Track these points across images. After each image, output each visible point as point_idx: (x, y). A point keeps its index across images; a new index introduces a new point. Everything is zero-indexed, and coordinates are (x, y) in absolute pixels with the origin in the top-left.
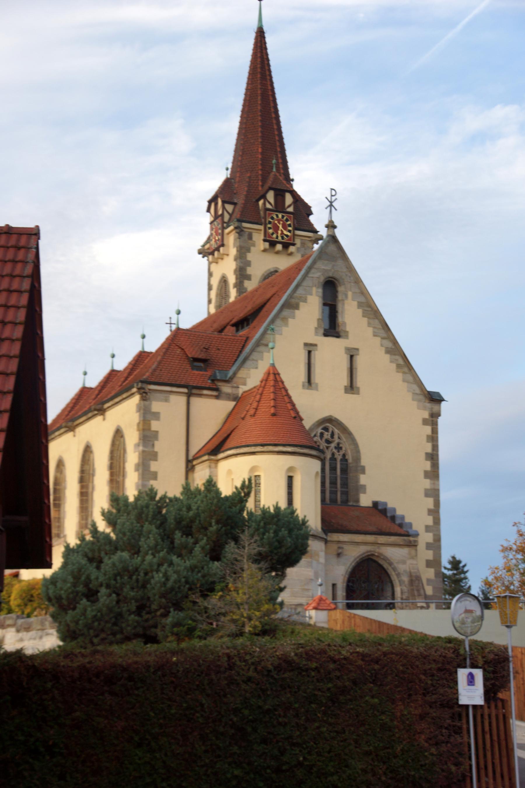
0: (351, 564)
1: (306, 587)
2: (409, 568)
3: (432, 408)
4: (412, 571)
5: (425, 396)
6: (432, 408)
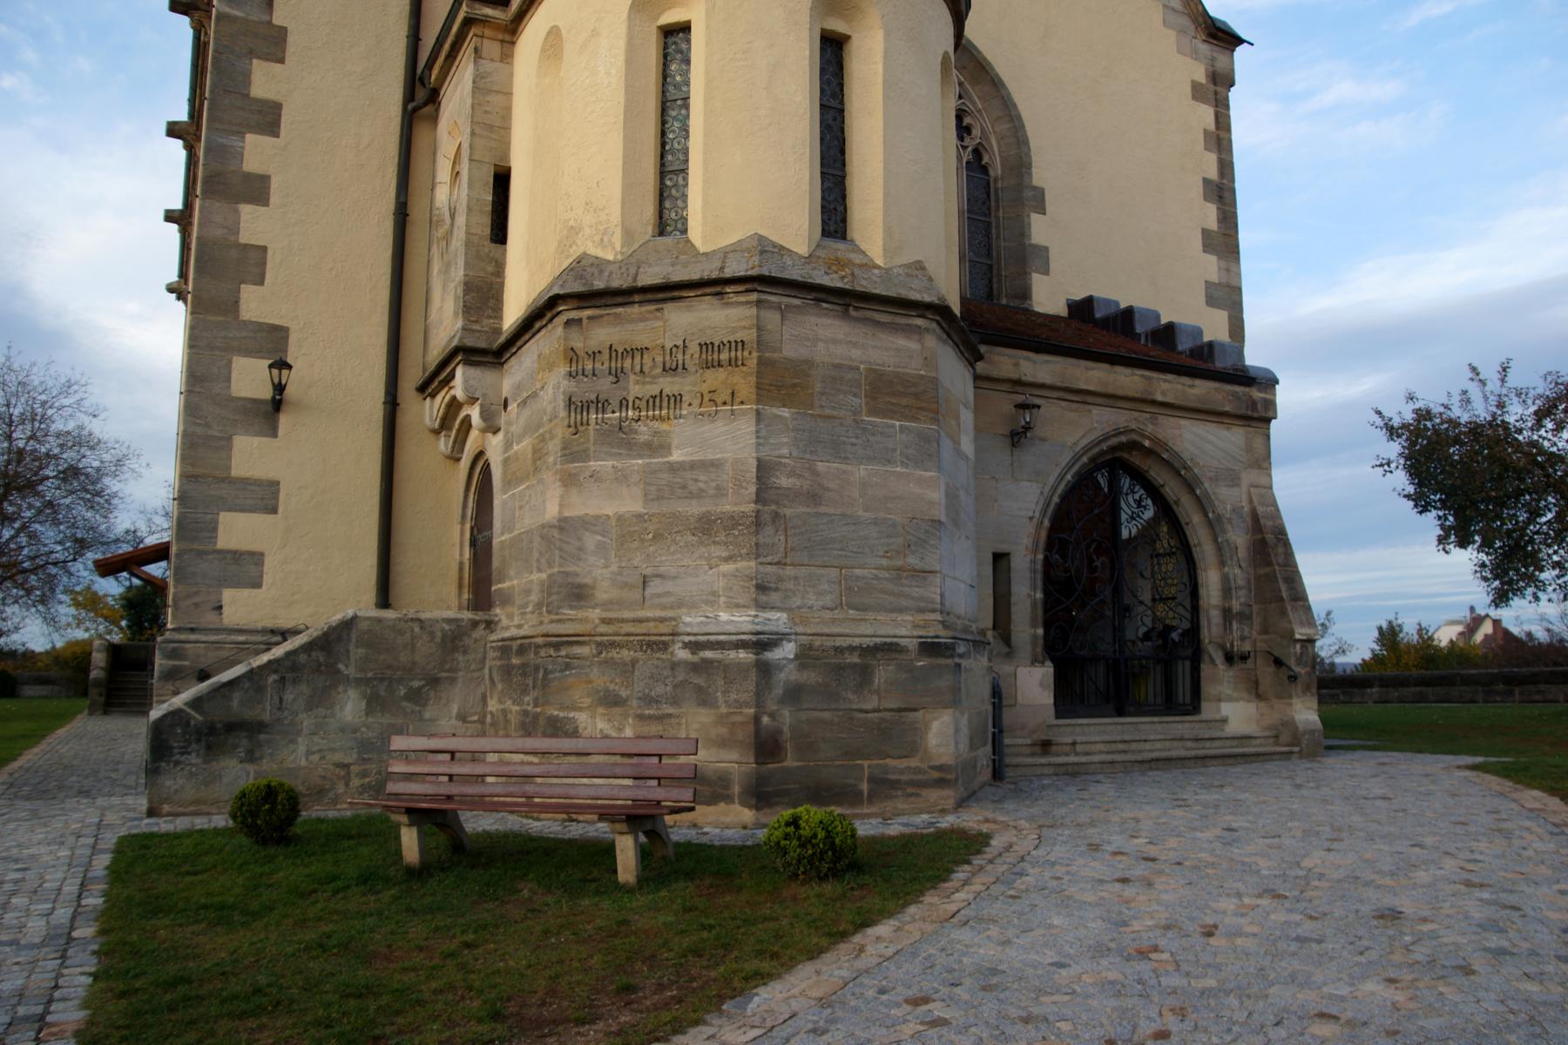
0: (1062, 477)
1: (912, 560)
2: (1251, 501)
3: (1213, 59)
4: (1260, 509)
5: (1194, 21)
6: (1213, 59)
